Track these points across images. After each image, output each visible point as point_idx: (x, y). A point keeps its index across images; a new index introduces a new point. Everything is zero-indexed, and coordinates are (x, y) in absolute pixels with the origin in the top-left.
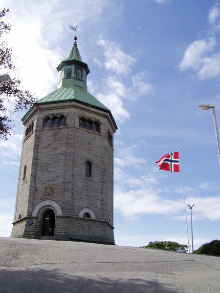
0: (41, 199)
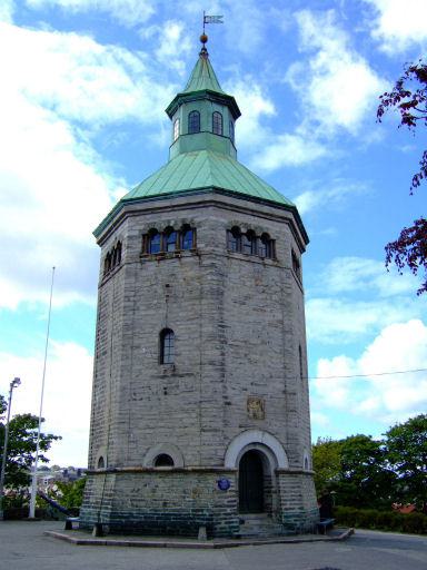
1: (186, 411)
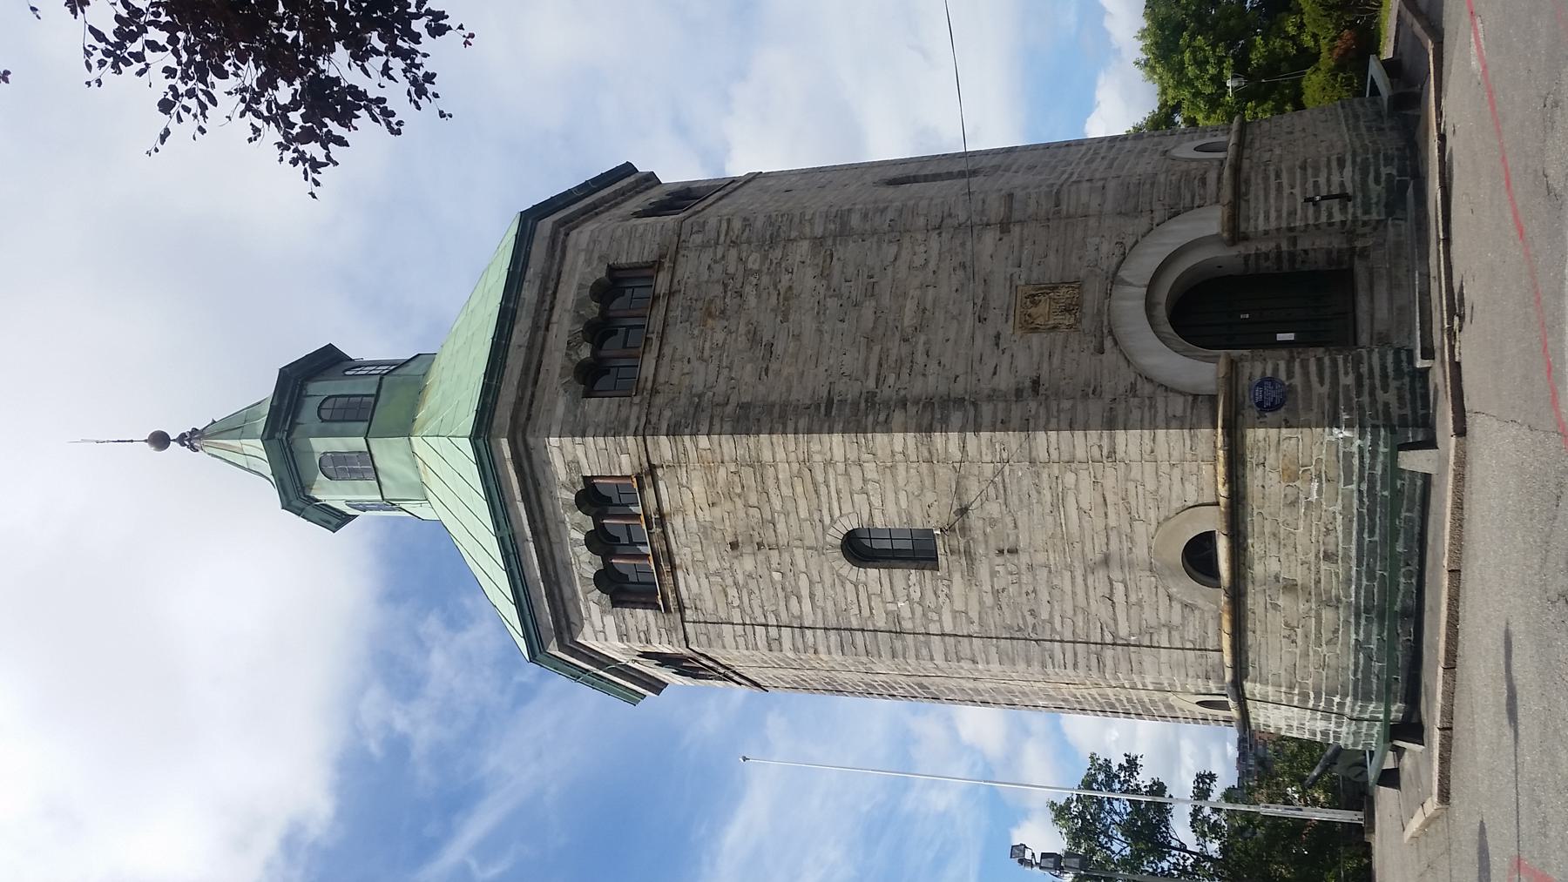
0: (1101, 351)
1: (1059, 502)
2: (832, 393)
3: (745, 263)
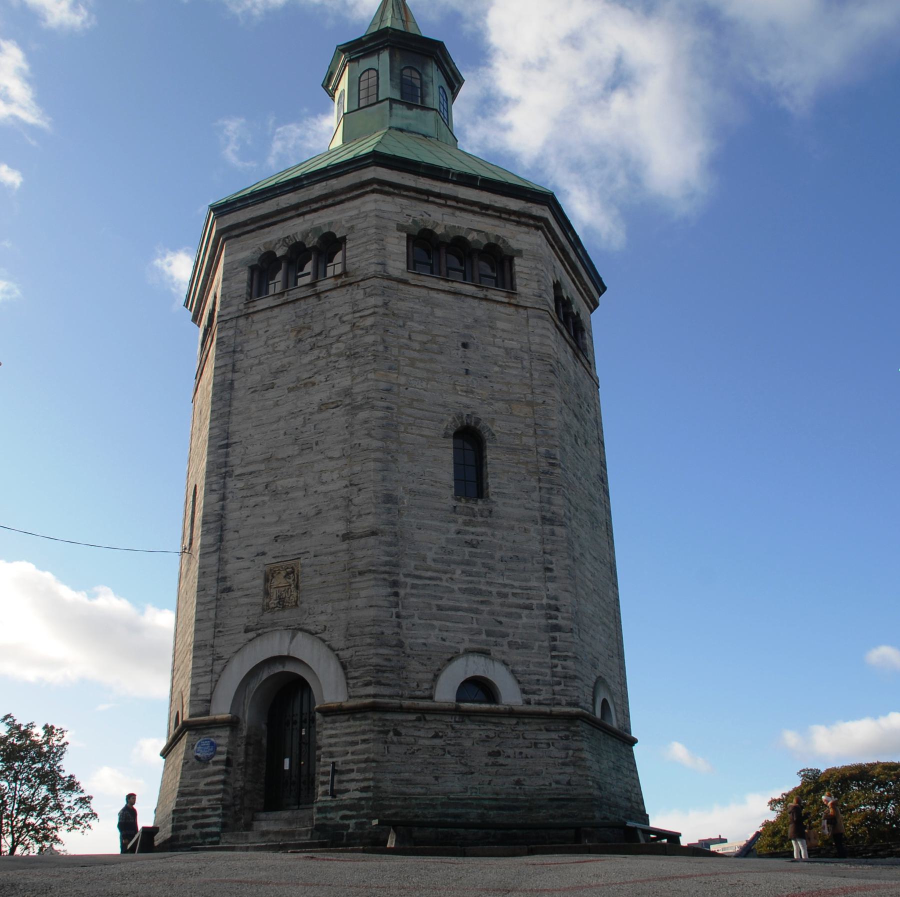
0: (247, 631)
2: (234, 445)
3: (338, 341)
